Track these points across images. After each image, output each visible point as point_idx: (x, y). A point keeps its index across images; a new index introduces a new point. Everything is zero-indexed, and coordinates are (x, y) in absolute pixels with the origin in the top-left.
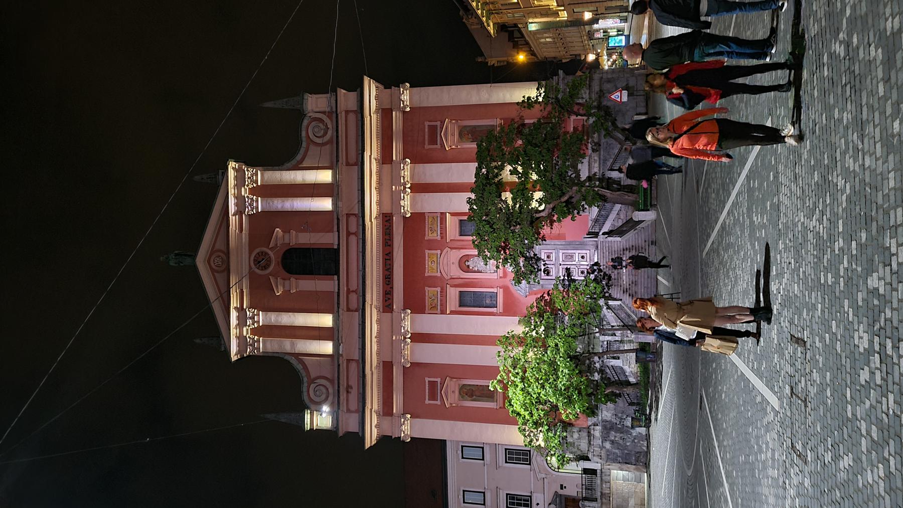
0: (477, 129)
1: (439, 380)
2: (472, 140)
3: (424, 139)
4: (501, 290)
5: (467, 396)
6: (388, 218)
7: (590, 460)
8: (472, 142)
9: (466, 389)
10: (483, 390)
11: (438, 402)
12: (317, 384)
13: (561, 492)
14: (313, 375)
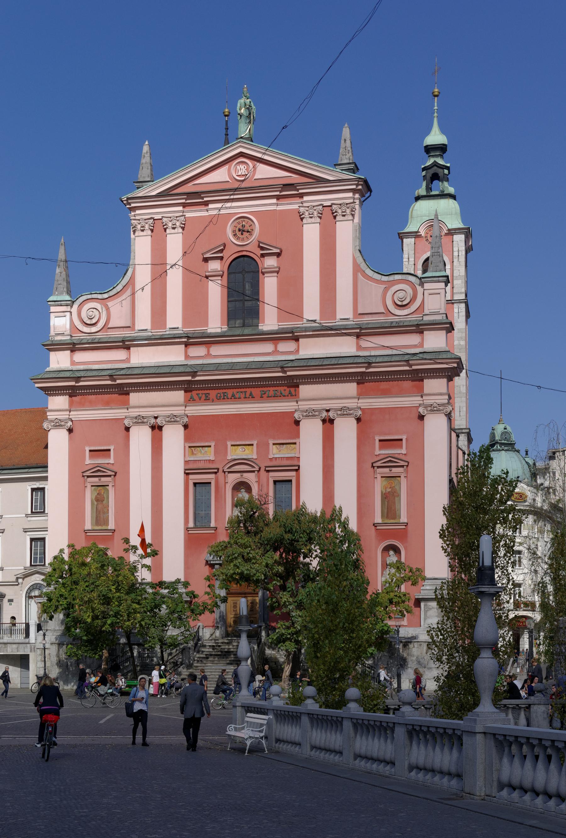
0: (396, 498)
1: (112, 461)
2: (384, 492)
3: (386, 434)
4: (213, 531)
5: (96, 494)
6: (294, 394)
7: (38, 632)
8: (382, 492)
9: (104, 493)
10: (104, 513)
11: (88, 461)
12: (100, 311)
13: (5, 600)
14: (110, 304)
